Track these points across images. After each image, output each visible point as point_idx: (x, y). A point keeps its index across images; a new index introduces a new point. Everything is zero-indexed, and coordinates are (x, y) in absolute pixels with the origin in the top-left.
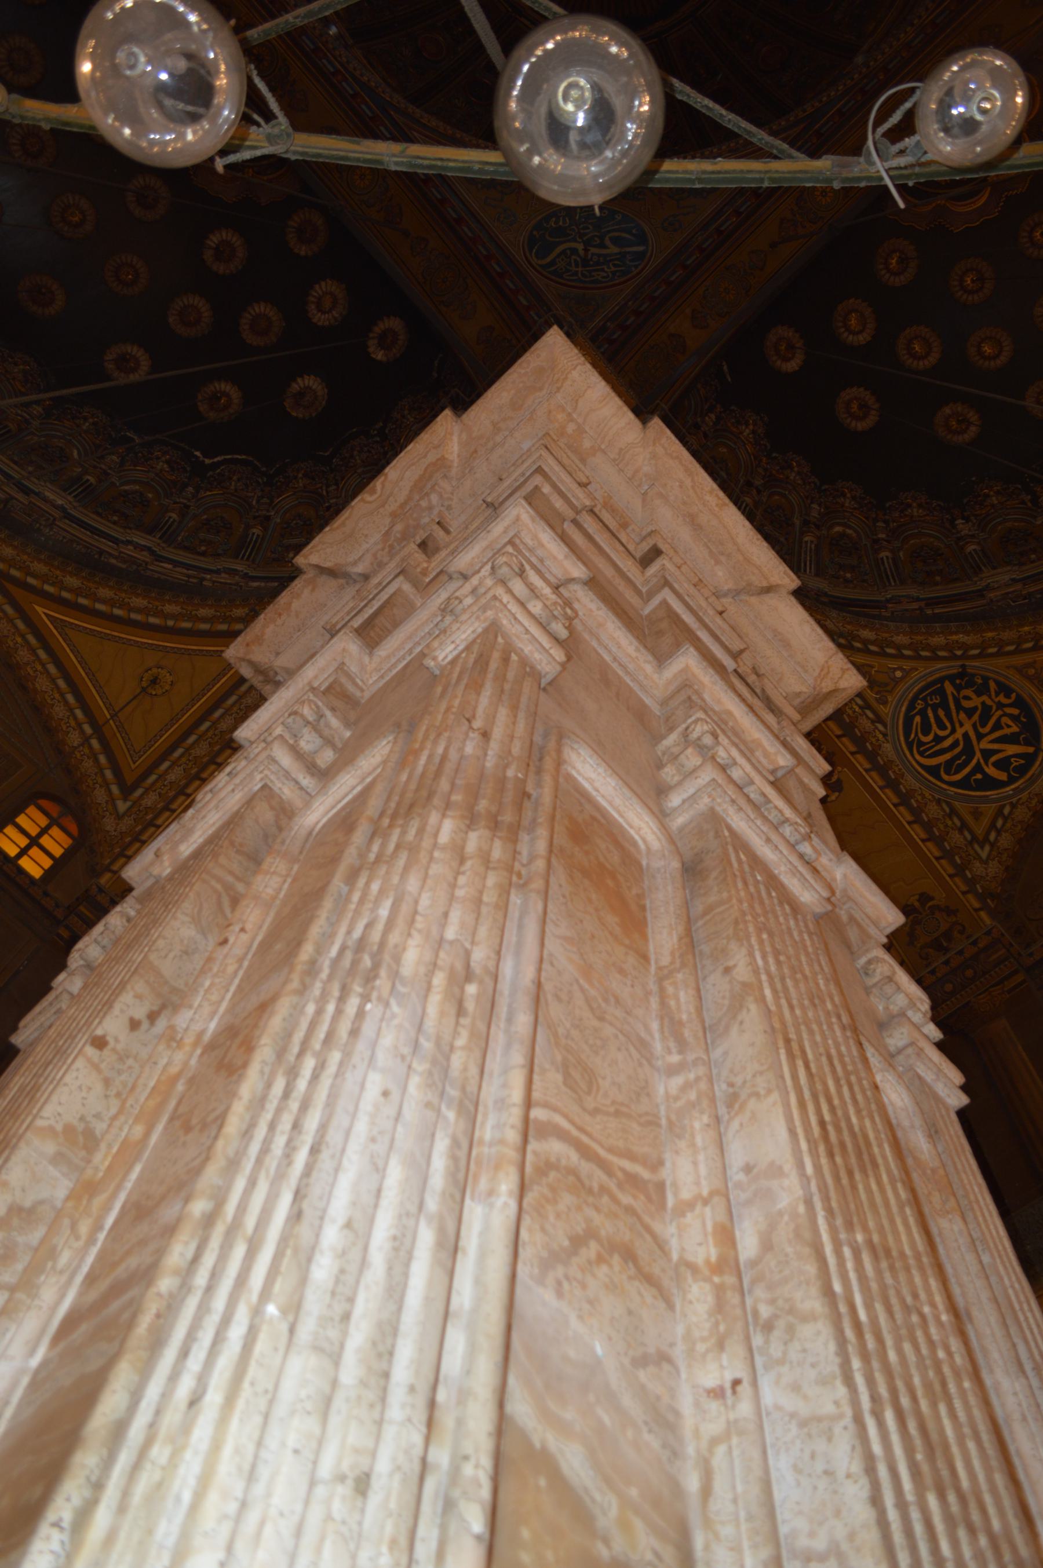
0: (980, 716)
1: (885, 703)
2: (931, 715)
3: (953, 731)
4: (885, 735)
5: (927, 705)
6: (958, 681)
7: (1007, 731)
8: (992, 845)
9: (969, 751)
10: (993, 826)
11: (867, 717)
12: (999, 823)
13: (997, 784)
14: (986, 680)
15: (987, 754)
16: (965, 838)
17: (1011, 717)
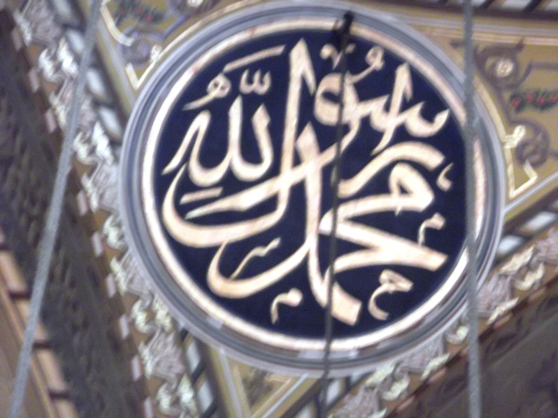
1: (141, 62)
2: (235, 112)
3: (274, 171)
4: (114, 143)
5: (235, 92)
6: (326, 51)
7: (393, 202)
9: (291, 232)
11: (88, 90)
14: (392, 61)
15: (332, 248)
17: (418, 166)
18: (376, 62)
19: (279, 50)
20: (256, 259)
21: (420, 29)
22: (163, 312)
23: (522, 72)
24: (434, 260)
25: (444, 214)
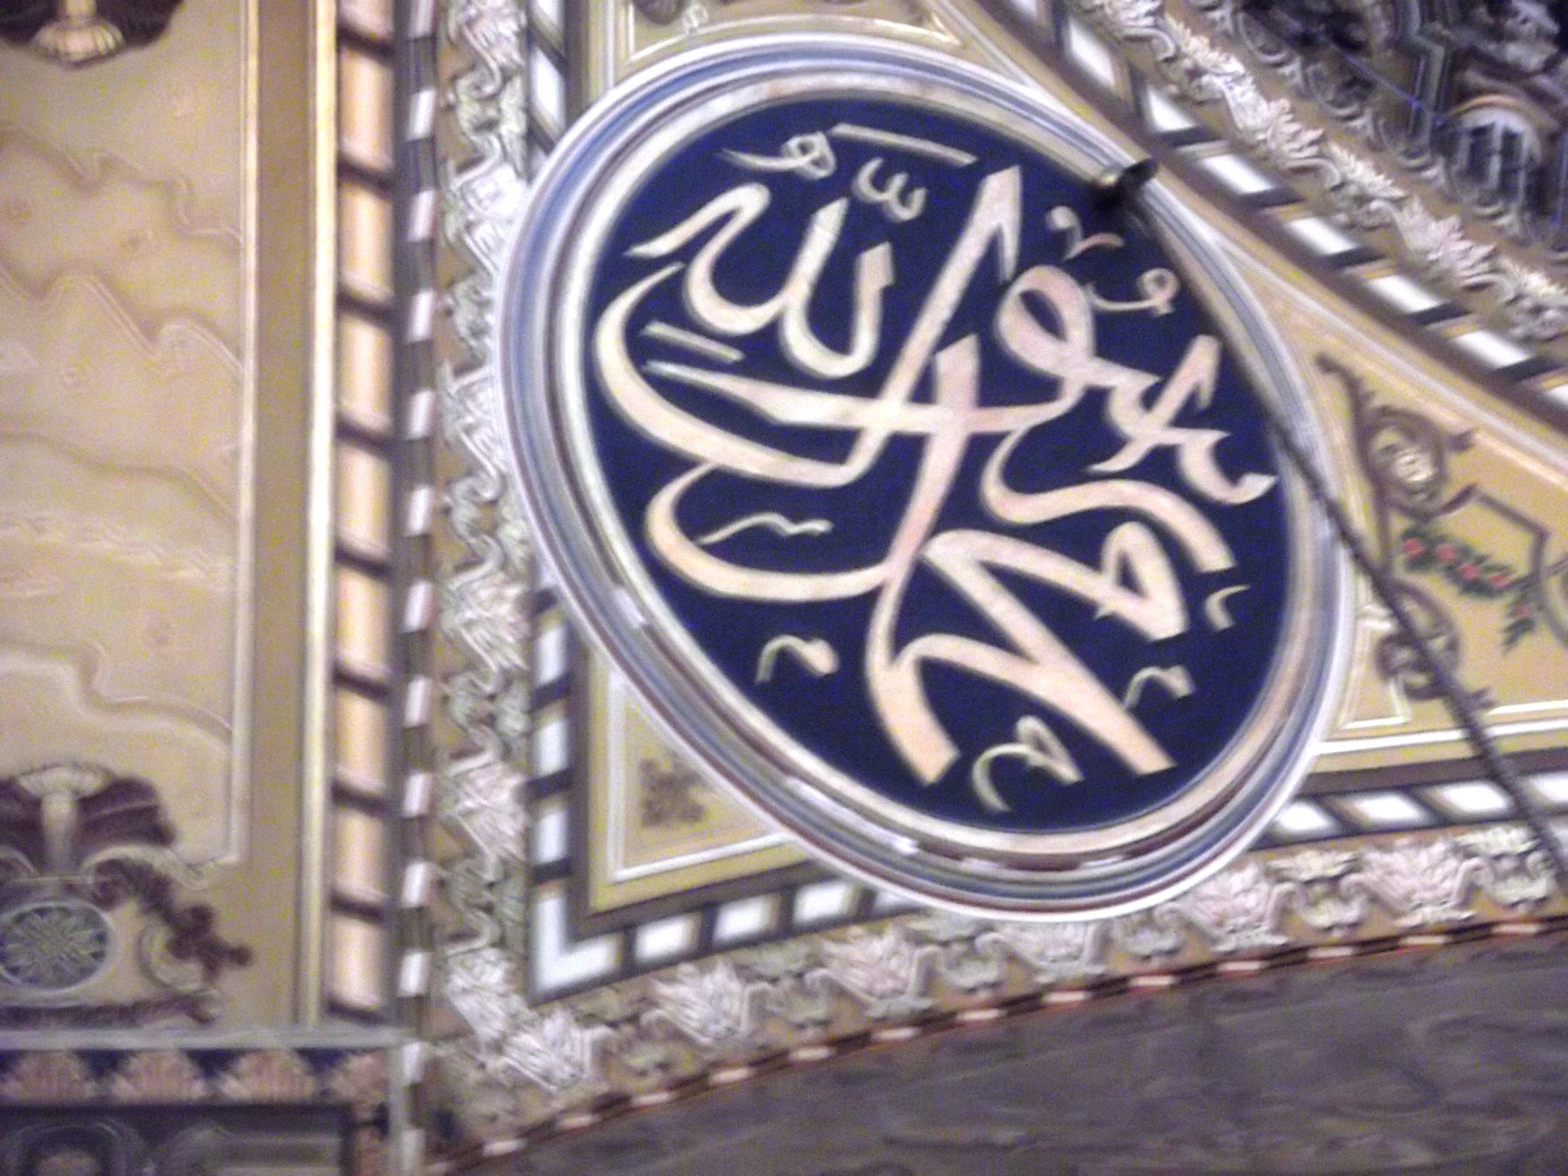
0: (1036, 435)
2: (826, 226)
3: (867, 384)
4: (537, 138)
6: (1062, 218)
7: (1096, 587)
8: (629, 968)
9: (863, 517)
10: (703, 903)
12: (742, 919)
13: (876, 762)
16: (529, 838)
18: (1157, 296)
19: (965, 159)
20: (763, 535)
21: (1266, 294)
22: (519, 526)
23: (1449, 493)
24: (1145, 756)
25: (1195, 675)
